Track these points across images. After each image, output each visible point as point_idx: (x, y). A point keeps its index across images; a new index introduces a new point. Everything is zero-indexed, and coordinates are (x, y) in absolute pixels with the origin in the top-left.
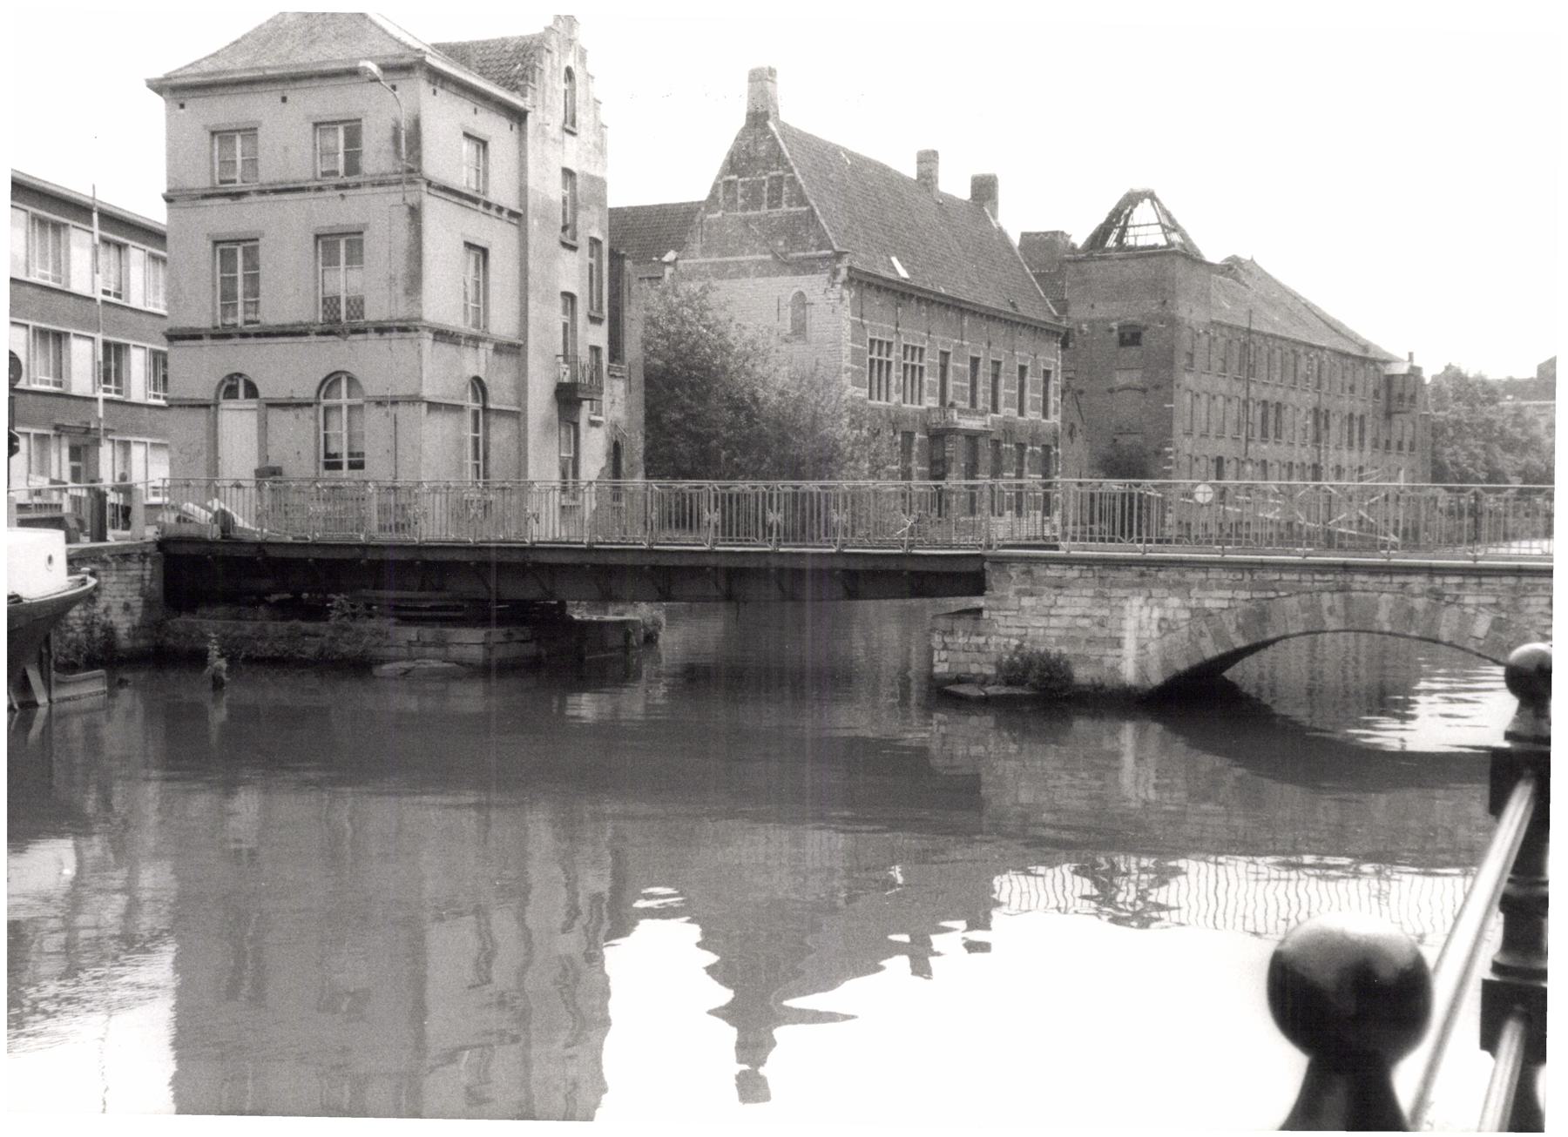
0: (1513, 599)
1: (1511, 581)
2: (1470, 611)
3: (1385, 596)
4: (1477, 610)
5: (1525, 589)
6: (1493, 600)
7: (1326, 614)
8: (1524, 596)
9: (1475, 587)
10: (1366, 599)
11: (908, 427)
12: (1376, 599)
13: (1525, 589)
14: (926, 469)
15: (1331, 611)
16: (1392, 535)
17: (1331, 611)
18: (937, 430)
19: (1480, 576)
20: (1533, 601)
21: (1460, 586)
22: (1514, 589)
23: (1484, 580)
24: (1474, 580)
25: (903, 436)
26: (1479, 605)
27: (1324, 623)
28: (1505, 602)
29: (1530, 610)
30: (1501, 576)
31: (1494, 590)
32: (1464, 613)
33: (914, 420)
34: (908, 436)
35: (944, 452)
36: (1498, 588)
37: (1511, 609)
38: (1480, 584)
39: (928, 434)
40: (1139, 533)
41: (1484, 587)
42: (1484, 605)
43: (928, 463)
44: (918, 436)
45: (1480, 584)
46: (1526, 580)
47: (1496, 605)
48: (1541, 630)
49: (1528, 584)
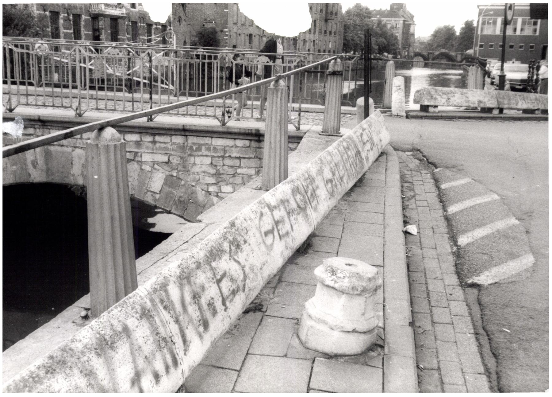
0: (181, 158)
1: (179, 139)
2: (147, 168)
3: (78, 151)
4: (153, 167)
5: (191, 148)
6: (165, 159)
7: (30, 166)
8: (191, 155)
9: (150, 145)
10: (63, 153)
11: (78, 12)
12: (70, 153)
13: (191, 148)
14: (90, 33)
15: (34, 164)
16: (170, 85)
17: (34, 164)
18: (94, 14)
19: (154, 135)
20: (198, 160)
21: (138, 144)
22: (183, 148)
23: (157, 138)
24: (149, 138)
25: (73, 16)
26: (154, 163)
27: (30, 175)
28: (175, 160)
29: (196, 169)
30: (171, 135)
31: (165, 149)
32: (142, 170)
33: (81, 8)
34: (77, 17)
35: (98, 25)
36: (169, 146)
37: (180, 168)
38: (154, 142)
39: (90, 16)
40: (12, 77)
41: (158, 145)
42: (158, 163)
43: (91, 28)
44: (84, 17)
45: (154, 142)
46: (192, 140)
47: (168, 163)
48: (205, 187)
49: (194, 143)
